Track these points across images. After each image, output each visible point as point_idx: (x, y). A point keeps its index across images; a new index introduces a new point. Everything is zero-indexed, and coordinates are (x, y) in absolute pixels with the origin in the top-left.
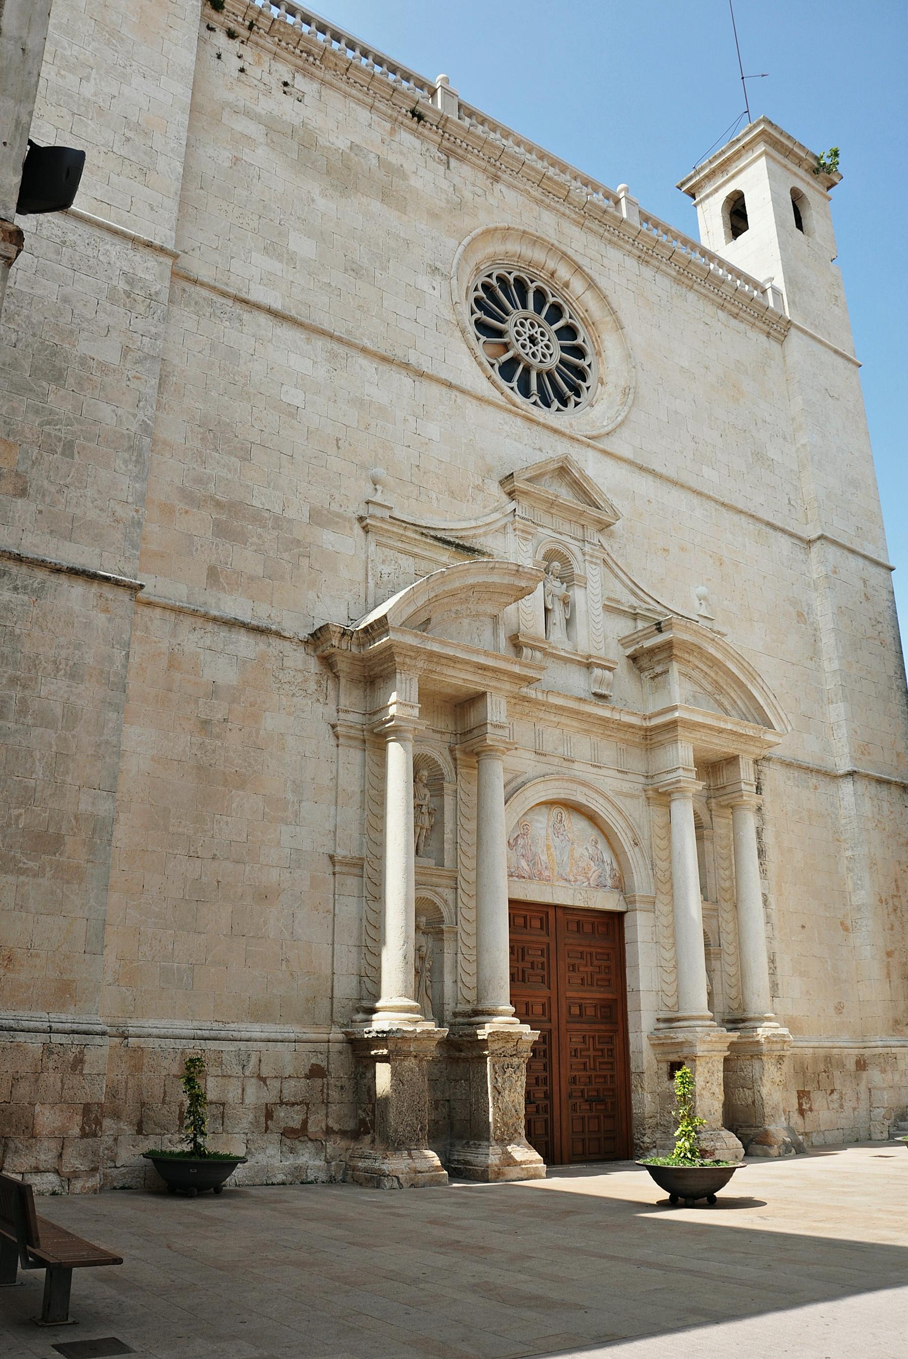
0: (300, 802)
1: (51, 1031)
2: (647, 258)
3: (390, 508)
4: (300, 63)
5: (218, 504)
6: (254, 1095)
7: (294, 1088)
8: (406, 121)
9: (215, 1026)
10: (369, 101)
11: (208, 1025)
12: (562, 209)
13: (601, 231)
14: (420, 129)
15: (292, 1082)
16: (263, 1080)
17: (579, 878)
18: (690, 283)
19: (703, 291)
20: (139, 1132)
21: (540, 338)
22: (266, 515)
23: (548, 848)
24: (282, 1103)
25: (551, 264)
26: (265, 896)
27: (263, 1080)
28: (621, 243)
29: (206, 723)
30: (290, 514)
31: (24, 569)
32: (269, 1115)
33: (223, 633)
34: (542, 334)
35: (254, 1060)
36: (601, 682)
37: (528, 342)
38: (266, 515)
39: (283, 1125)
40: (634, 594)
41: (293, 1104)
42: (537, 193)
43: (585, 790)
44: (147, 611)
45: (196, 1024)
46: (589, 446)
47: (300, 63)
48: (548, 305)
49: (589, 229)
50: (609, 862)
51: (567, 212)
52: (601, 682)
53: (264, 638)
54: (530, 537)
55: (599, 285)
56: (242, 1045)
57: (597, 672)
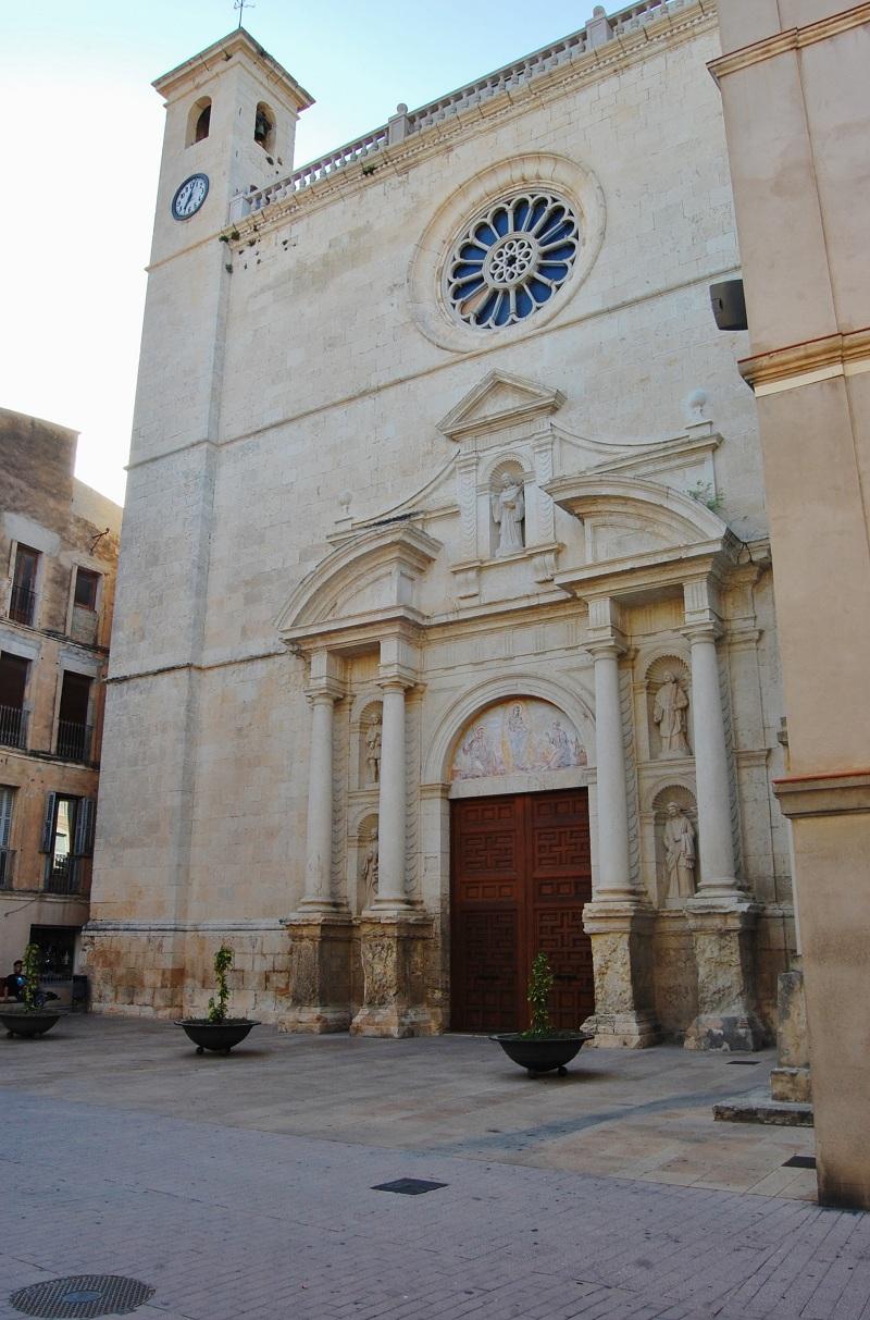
0: (292, 764)
1: (150, 930)
2: (625, 63)
3: (351, 518)
4: (289, 218)
5: (247, 583)
6: (262, 965)
7: (281, 962)
8: (366, 182)
9: (245, 921)
10: (337, 196)
11: (239, 921)
12: (514, 113)
13: (561, 91)
14: (377, 176)
15: (280, 957)
16: (264, 955)
17: (537, 764)
18: (689, 33)
19: (709, 25)
20: (203, 986)
21: (505, 257)
22: (273, 573)
23: (503, 744)
24: (274, 971)
25: (517, 174)
26: (271, 834)
27: (264, 955)
28: (587, 80)
29: (240, 730)
30: (287, 565)
31: (144, 679)
32: (267, 979)
33: (249, 667)
34: (500, 255)
35: (259, 942)
36: (545, 568)
37: (517, 264)
38: (273, 573)
39: (275, 985)
40: (600, 452)
41: (281, 972)
42: (486, 124)
43: (526, 681)
44: (210, 673)
45: (233, 921)
46: (542, 334)
47: (289, 218)
48: (492, 226)
49: (550, 101)
50: (574, 740)
51: (521, 110)
52: (545, 568)
53: (271, 660)
54: (474, 467)
55: (558, 153)
56: (253, 933)
57: (537, 560)
